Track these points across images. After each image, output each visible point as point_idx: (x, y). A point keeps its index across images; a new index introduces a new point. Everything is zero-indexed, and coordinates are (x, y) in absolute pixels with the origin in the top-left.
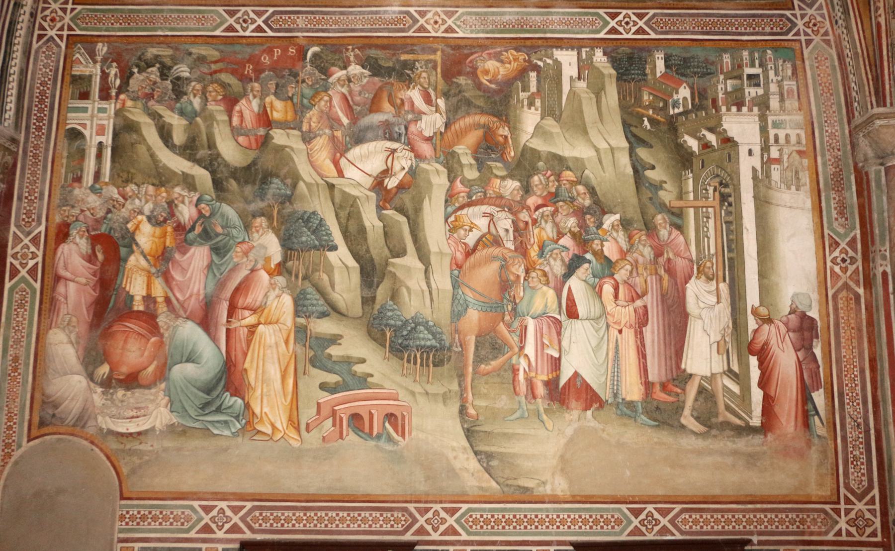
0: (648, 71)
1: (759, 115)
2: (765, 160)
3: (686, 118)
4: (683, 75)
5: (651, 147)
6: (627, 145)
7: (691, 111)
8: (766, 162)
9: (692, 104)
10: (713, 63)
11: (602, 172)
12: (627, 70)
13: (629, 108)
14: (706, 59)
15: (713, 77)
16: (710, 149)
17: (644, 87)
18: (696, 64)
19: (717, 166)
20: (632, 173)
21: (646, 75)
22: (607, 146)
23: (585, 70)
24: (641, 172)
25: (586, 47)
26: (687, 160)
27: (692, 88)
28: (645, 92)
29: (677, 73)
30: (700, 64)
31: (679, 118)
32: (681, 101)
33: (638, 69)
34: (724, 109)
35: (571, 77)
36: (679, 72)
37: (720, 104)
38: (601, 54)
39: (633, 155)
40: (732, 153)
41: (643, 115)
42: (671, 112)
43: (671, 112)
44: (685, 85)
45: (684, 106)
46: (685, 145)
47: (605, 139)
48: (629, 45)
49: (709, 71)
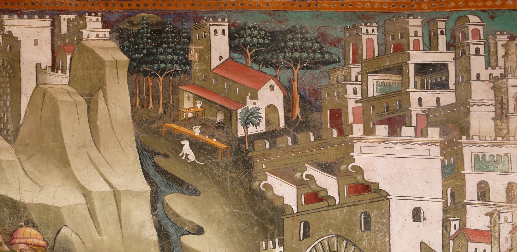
0: (193, 55)
1: (442, 143)
2: (453, 232)
3: (273, 145)
4: (267, 64)
5: (196, 193)
6: (148, 188)
7: (283, 132)
8: (456, 236)
9: (287, 119)
10: (335, 43)
11: (95, 233)
12: (150, 53)
13: (153, 122)
14: (323, 36)
15: (335, 70)
16: (324, 204)
17: (184, 85)
18: (298, 43)
19: (338, 236)
20: (155, 238)
21: (188, 63)
22: (106, 188)
23: (67, 52)
24: (174, 238)
25: (68, 13)
26: (272, 222)
27: (287, 90)
28: (186, 95)
29: (255, 61)
30: (308, 44)
31: (258, 144)
32: (262, 112)
33: (174, 53)
34: (358, 129)
35: (38, 66)
36: (261, 58)
37: (351, 120)
38: (99, 25)
39: (159, 206)
40: (374, 214)
41: (181, 136)
42: (241, 132)
43: (241, 132)
44: (272, 82)
45: (268, 122)
46: (269, 194)
47: (102, 176)
48: (157, 7)
49: (327, 56)
